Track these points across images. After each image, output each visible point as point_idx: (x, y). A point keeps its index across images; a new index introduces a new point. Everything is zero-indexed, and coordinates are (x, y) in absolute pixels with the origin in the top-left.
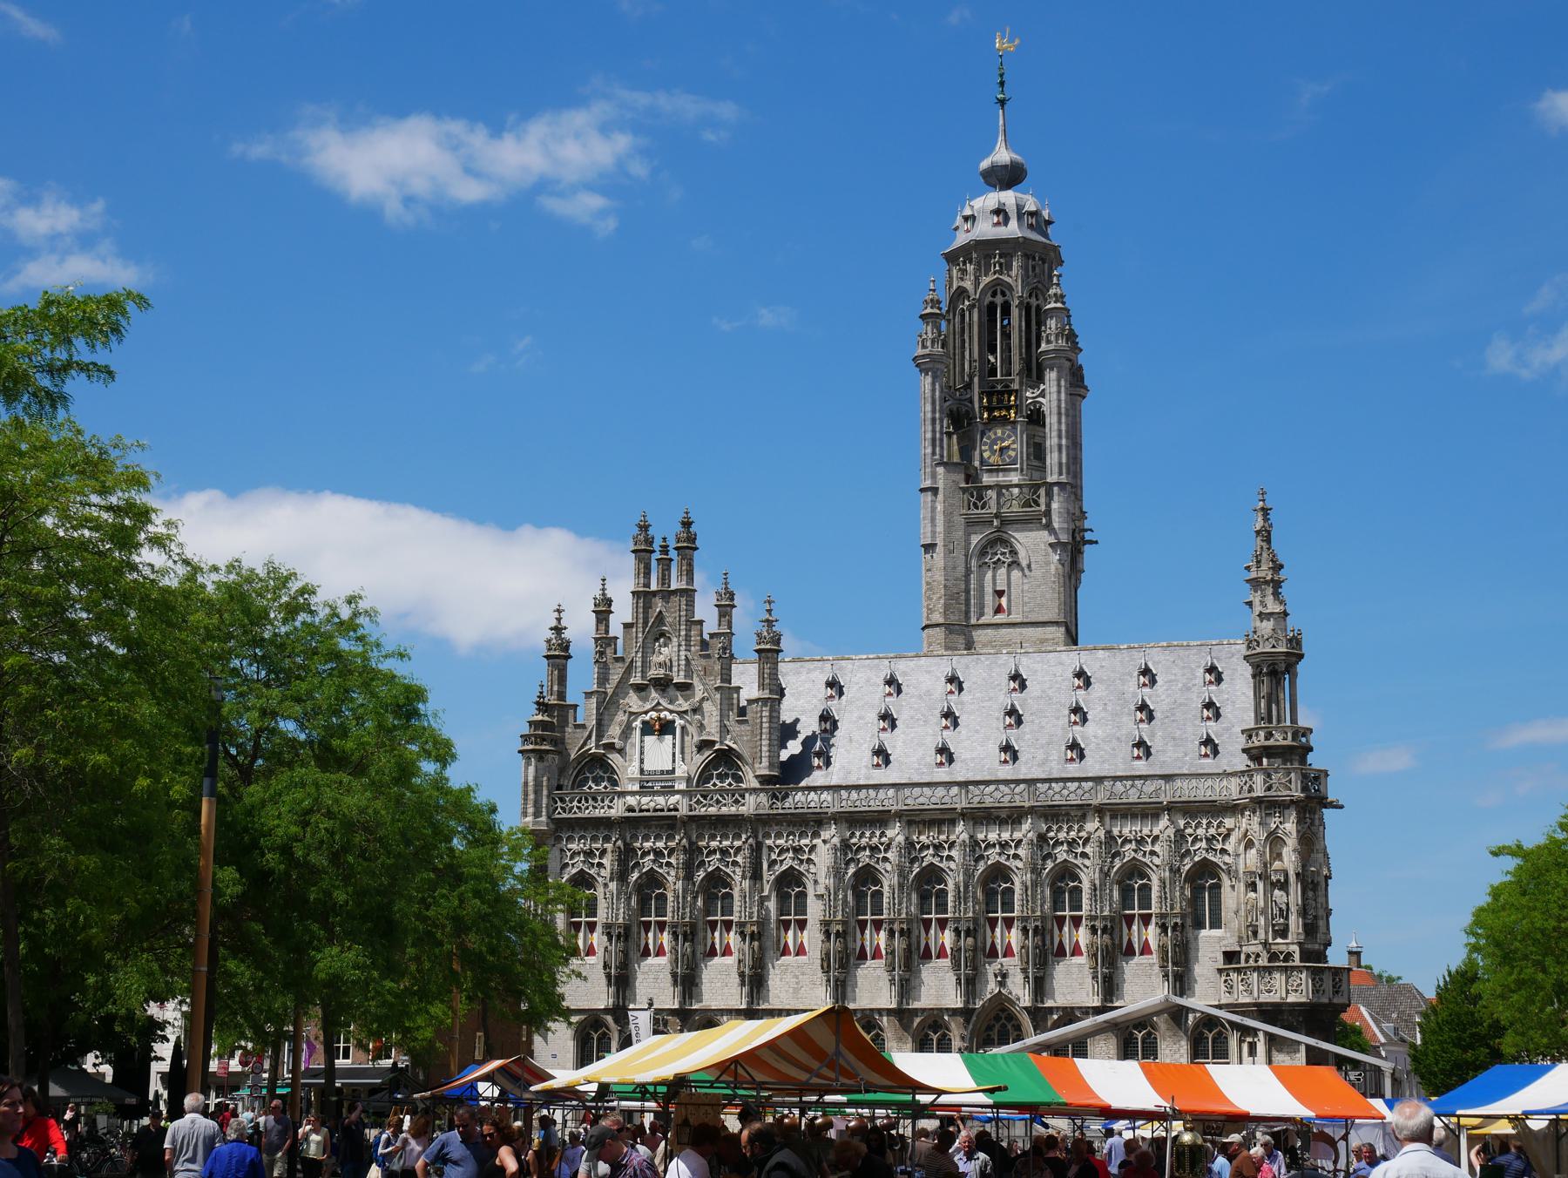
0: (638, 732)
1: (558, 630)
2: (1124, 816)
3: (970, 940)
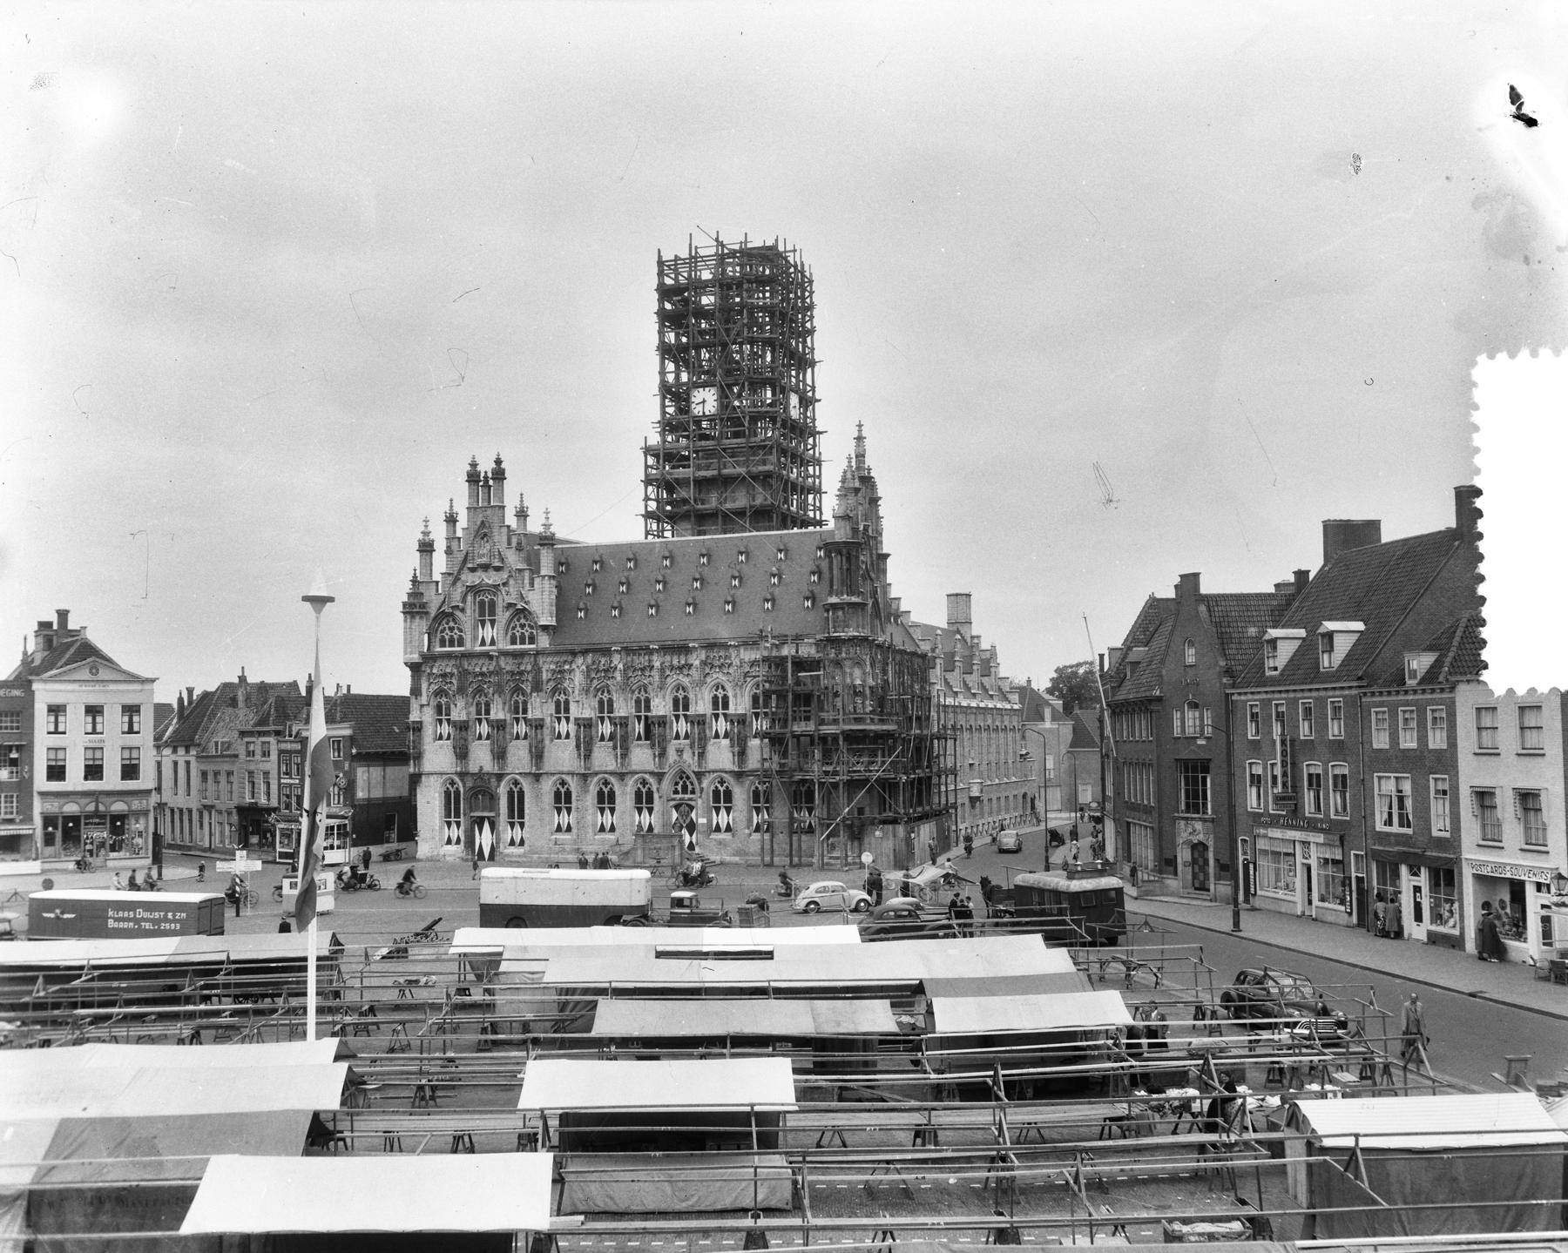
1: (426, 534)
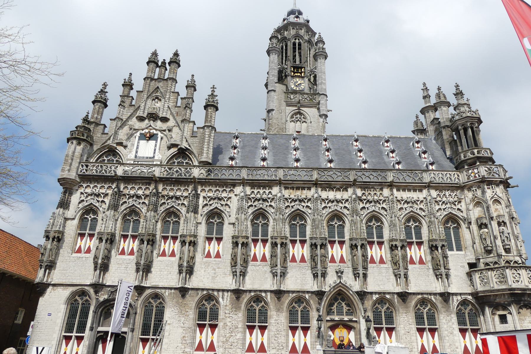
0: (137, 138)
2: (404, 190)
3: (322, 250)
